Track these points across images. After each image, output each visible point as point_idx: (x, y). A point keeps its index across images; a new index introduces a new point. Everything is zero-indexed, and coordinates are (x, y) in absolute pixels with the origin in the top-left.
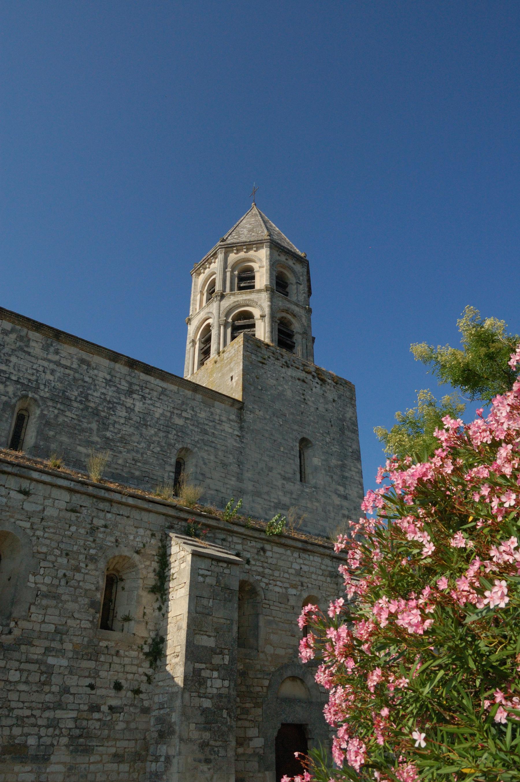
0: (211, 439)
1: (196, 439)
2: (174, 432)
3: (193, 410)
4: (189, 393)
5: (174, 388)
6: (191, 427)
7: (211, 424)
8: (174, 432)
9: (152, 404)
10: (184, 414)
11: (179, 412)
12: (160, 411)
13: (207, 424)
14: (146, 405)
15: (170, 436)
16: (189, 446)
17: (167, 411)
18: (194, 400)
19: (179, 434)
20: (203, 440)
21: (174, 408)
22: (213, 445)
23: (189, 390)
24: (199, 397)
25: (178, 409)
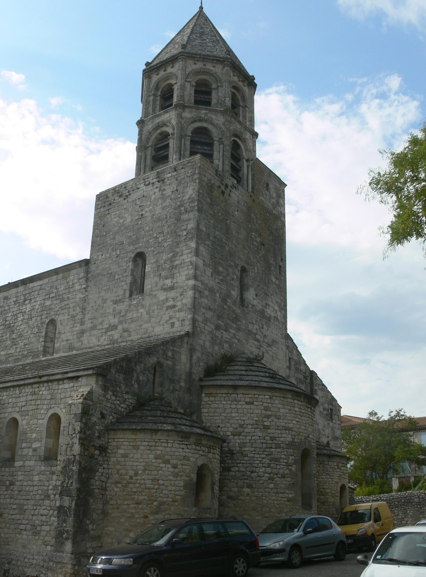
0: (66, 303)
1: (58, 309)
2: (45, 312)
3: (56, 289)
4: (54, 278)
5: (46, 280)
6: (55, 302)
7: (67, 291)
8: (45, 312)
9: (34, 302)
10: (52, 295)
11: (48, 296)
12: (38, 303)
13: (64, 293)
14: (32, 304)
15: (43, 317)
16: (53, 317)
17: (42, 300)
18: (58, 280)
19: (48, 312)
20: (61, 307)
21: (45, 295)
22: (67, 306)
23: (55, 275)
24: (60, 276)
25: (47, 294)
